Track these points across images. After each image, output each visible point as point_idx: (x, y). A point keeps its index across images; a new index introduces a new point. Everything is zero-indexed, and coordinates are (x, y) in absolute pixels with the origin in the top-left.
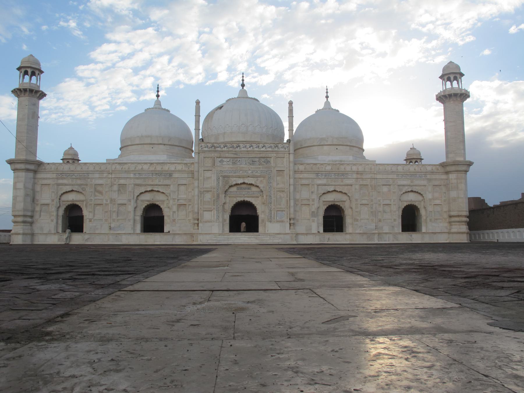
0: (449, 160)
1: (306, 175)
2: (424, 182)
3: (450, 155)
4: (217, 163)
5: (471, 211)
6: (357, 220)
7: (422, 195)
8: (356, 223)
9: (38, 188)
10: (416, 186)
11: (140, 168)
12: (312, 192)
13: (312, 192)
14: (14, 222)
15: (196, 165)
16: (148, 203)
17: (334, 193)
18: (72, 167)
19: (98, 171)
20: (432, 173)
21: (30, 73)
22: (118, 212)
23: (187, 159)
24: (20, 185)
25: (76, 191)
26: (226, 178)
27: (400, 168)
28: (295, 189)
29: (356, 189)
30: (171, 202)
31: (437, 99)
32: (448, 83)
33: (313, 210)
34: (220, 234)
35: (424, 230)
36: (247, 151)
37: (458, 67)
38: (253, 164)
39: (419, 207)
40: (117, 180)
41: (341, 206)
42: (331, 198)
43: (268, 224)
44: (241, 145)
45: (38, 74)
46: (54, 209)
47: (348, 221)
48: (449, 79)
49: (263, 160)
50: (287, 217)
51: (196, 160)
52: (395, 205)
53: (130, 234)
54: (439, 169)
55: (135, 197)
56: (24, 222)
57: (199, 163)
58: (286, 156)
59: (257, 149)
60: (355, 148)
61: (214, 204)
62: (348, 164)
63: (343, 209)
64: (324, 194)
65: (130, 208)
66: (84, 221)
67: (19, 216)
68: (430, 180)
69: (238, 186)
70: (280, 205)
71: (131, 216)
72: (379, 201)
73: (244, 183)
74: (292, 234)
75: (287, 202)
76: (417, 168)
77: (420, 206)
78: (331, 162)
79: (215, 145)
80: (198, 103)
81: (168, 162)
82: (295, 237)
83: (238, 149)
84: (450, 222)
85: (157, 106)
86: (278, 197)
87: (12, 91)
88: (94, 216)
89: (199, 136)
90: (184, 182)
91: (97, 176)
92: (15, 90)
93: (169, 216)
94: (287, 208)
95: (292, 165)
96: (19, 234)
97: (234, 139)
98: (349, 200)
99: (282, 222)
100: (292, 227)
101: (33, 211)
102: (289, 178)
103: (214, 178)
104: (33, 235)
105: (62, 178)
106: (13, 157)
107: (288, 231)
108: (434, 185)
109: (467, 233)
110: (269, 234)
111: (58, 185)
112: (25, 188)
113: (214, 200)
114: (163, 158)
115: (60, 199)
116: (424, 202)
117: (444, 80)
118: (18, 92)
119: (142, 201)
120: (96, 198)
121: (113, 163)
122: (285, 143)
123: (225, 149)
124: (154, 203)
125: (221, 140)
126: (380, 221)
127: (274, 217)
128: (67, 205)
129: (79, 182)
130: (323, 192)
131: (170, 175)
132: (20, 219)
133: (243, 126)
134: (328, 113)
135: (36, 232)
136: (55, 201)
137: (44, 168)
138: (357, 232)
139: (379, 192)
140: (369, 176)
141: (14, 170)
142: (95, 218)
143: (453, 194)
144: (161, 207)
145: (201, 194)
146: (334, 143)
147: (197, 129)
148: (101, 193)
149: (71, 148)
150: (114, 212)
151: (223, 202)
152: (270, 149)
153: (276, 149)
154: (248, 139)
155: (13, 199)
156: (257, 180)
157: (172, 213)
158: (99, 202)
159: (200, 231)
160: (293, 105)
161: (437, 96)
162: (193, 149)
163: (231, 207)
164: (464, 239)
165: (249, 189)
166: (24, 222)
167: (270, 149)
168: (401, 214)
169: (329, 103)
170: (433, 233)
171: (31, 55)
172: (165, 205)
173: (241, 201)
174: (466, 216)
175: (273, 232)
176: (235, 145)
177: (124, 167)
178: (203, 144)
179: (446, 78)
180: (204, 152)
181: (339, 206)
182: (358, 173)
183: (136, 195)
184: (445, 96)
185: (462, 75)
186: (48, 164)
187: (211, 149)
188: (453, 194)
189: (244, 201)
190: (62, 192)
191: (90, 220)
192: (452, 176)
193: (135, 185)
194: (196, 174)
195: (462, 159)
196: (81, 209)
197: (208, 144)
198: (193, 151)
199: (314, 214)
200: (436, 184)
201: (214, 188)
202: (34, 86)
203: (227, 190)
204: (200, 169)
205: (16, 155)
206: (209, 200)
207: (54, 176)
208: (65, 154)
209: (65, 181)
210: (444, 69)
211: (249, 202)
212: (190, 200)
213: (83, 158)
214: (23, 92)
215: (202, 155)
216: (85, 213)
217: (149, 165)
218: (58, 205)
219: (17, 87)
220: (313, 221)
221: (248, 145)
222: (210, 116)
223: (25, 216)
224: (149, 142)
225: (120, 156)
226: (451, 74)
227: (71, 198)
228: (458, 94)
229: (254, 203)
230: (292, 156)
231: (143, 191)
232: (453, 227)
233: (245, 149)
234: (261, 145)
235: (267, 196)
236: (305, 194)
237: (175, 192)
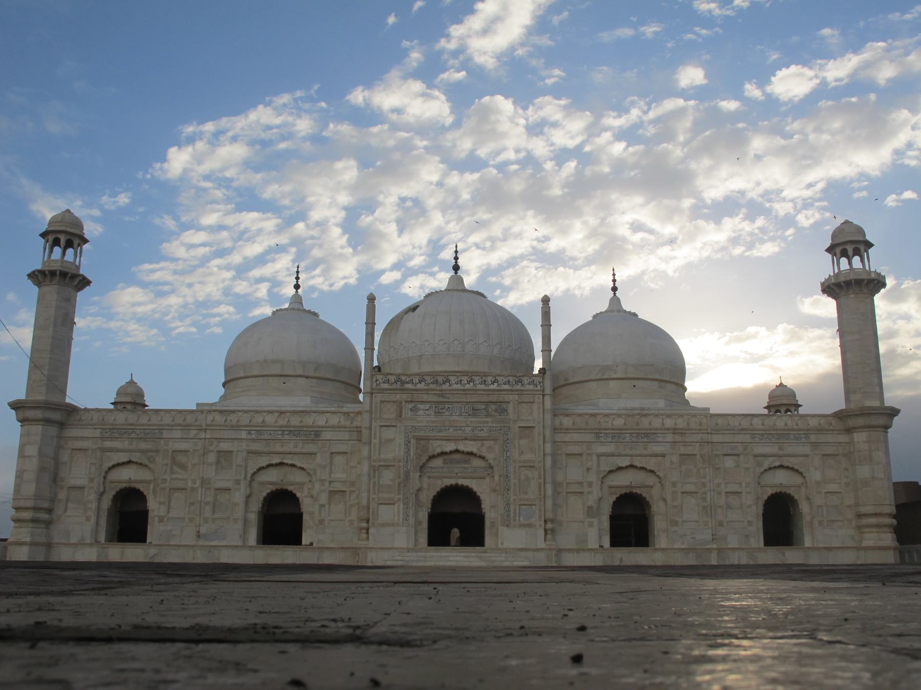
0: (852, 406)
1: (575, 437)
2: (806, 450)
3: (853, 397)
4: (407, 413)
5: (898, 507)
6: (675, 523)
7: (801, 473)
8: (675, 528)
9: (65, 457)
10: (789, 456)
11: (260, 420)
12: (588, 469)
13: (588, 469)
14: (16, 520)
15: (366, 416)
16: (274, 488)
17: (631, 471)
18: (132, 418)
19: (180, 425)
20: (819, 430)
21: (63, 242)
22: (214, 505)
23: (349, 405)
24: (32, 450)
25: (137, 463)
27: (757, 422)
28: (554, 463)
29: (672, 463)
30: (317, 486)
32: (844, 261)
33: (590, 503)
34: (409, 550)
35: (808, 542)
36: (464, 390)
37: (860, 231)
38: (474, 415)
39: (796, 497)
40: (215, 443)
41: (644, 495)
42: (624, 481)
43: (504, 532)
44: (452, 379)
45: (79, 245)
46: (93, 497)
47: (659, 524)
48: (844, 254)
49: (493, 407)
50: (540, 517)
51: (367, 407)
52: (749, 493)
53: (236, 547)
54: (833, 422)
55: (249, 476)
56: (34, 521)
57: (371, 412)
58: (538, 399)
59: (482, 387)
60: (668, 385)
61: (399, 490)
62: (657, 416)
63: (648, 502)
64: (611, 472)
65: (239, 497)
66: (150, 521)
67: (26, 509)
68: (815, 445)
69: (446, 457)
70: (526, 493)
71: (240, 512)
72: (719, 485)
73: (457, 451)
74: (550, 549)
76: (789, 423)
77: (799, 496)
78: (623, 412)
79: (403, 378)
80: (371, 299)
81: (314, 409)
82: (556, 555)
83: (446, 387)
84: (859, 528)
85: (296, 306)
87: (29, 276)
88: (168, 512)
89: (372, 360)
90: (344, 448)
91: (178, 434)
92: (33, 272)
93: (311, 514)
94: (540, 500)
95: (548, 416)
96: (22, 544)
97: (438, 368)
98: (658, 485)
99: (530, 526)
100: (549, 536)
101: (53, 500)
102: (544, 442)
104: (49, 546)
105: (112, 439)
106: (22, 397)
107: (542, 545)
108: (824, 455)
109: (895, 549)
110: (506, 551)
111: (104, 450)
112: (41, 454)
114: (303, 402)
115: (105, 478)
116: (807, 487)
117: (835, 254)
118: (39, 277)
119: (262, 484)
120: (175, 476)
121: (209, 411)
122: (535, 375)
123: (422, 386)
124: (285, 487)
125: (414, 369)
126: (721, 524)
127: (514, 517)
128: (118, 489)
129: (143, 445)
130: (608, 469)
131: (315, 434)
132: (27, 515)
133: (456, 342)
134: (616, 317)
135: (56, 540)
136: (96, 481)
137: (78, 417)
138: (676, 546)
139: (718, 469)
140: (698, 438)
141: (23, 421)
142: (170, 515)
143: (864, 472)
144: (298, 495)
145: (374, 472)
146: (629, 375)
147: (369, 348)
148: (183, 467)
149: (132, 383)
150: (207, 503)
151: (417, 488)
152: (507, 387)
153: (519, 387)
154: (465, 368)
155: (17, 477)
156: (482, 445)
157: (317, 507)
158: (179, 484)
159: (371, 543)
161: (822, 284)
162: (362, 386)
163: (431, 497)
164: (890, 558)
165: (466, 462)
166: (34, 521)
167: (507, 387)
168: (761, 512)
169: (618, 300)
170: (826, 548)
171: (68, 211)
172: (306, 492)
173: (451, 485)
174: (890, 515)
175: (512, 546)
176: (440, 379)
177: (229, 418)
178: (379, 377)
179: (838, 250)
181: (641, 495)
182: (675, 431)
183: (251, 472)
184: (838, 285)
185: (869, 245)
186: (86, 410)
187: (394, 386)
188: (864, 472)
189: (457, 485)
190: (110, 464)
191: (161, 520)
192: (860, 437)
193: (249, 452)
194: (365, 433)
195: (876, 404)
196: (145, 497)
197: (389, 377)
198: (360, 391)
199: (591, 512)
200: (828, 452)
201: (400, 461)
203: (424, 464)
204: (374, 424)
205: (27, 394)
206: (390, 483)
207: (97, 433)
208: (119, 393)
209: (116, 444)
210: (834, 237)
211: (467, 487)
212: (353, 484)
213: (152, 402)
214: (49, 277)
215: (378, 398)
216: (153, 506)
217: (277, 415)
218: (102, 489)
219: (39, 267)
220: (591, 525)
221: (465, 379)
222: (394, 325)
223: (36, 509)
224: (278, 371)
225: (223, 398)
226: (849, 243)
227: (127, 476)
228: (863, 280)
229: (475, 489)
230: (548, 401)
231: (264, 465)
232: (866, 535)
233: (459, 387)
234: (489, 379)
235: (500, 476)
236: (573, 472)
237: (324, 467)
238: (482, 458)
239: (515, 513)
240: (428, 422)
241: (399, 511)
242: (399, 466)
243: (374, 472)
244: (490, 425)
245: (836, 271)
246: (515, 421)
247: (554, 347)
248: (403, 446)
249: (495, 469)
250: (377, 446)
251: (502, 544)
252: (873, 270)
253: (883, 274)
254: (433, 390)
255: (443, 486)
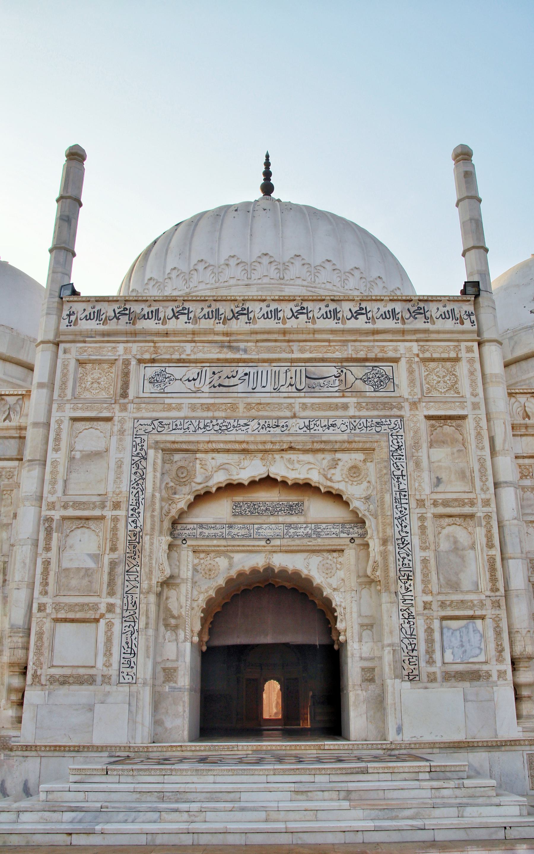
26: (177, 457)
36: (284, 332)
44: (255, 308)
49: (359, 371)
50: (500, 651)
58: (467, 352)
61: (111, 583)
73: (268, 482)
75: (492, 569)
79: (136, 308)
86: (444, 546)
94: (496, 605)
103: (122, 452)
107: (509, 728)
113: (113, 565)
127: (430, 652)
145: (49, 532)
151: (157, 577)
152: (390, 324)
163: (201, 602)
165: (292, 509)
173: (254, 571)
175: (428, 738)
178: (78, 307)
180: (83, 337)
187: (112, 326)
189: (269, 569)
201: (117, 506)
203: (182, 513)
204: (55, 415)
206: (91, 564)
211: (297, 574)
235: (385, 542)
238: (336, 497)
239: (430, 641)
240: (193, 408)
241: (109, 640)
242: (115, 519)
243: (49, 532)
244: (352, 412)
246: (414, 405)
248: (126, 467)
249: (370, 523)
250: (61, 469)
251: (399, 730)
254: (206, 332)
255: (233, 573)
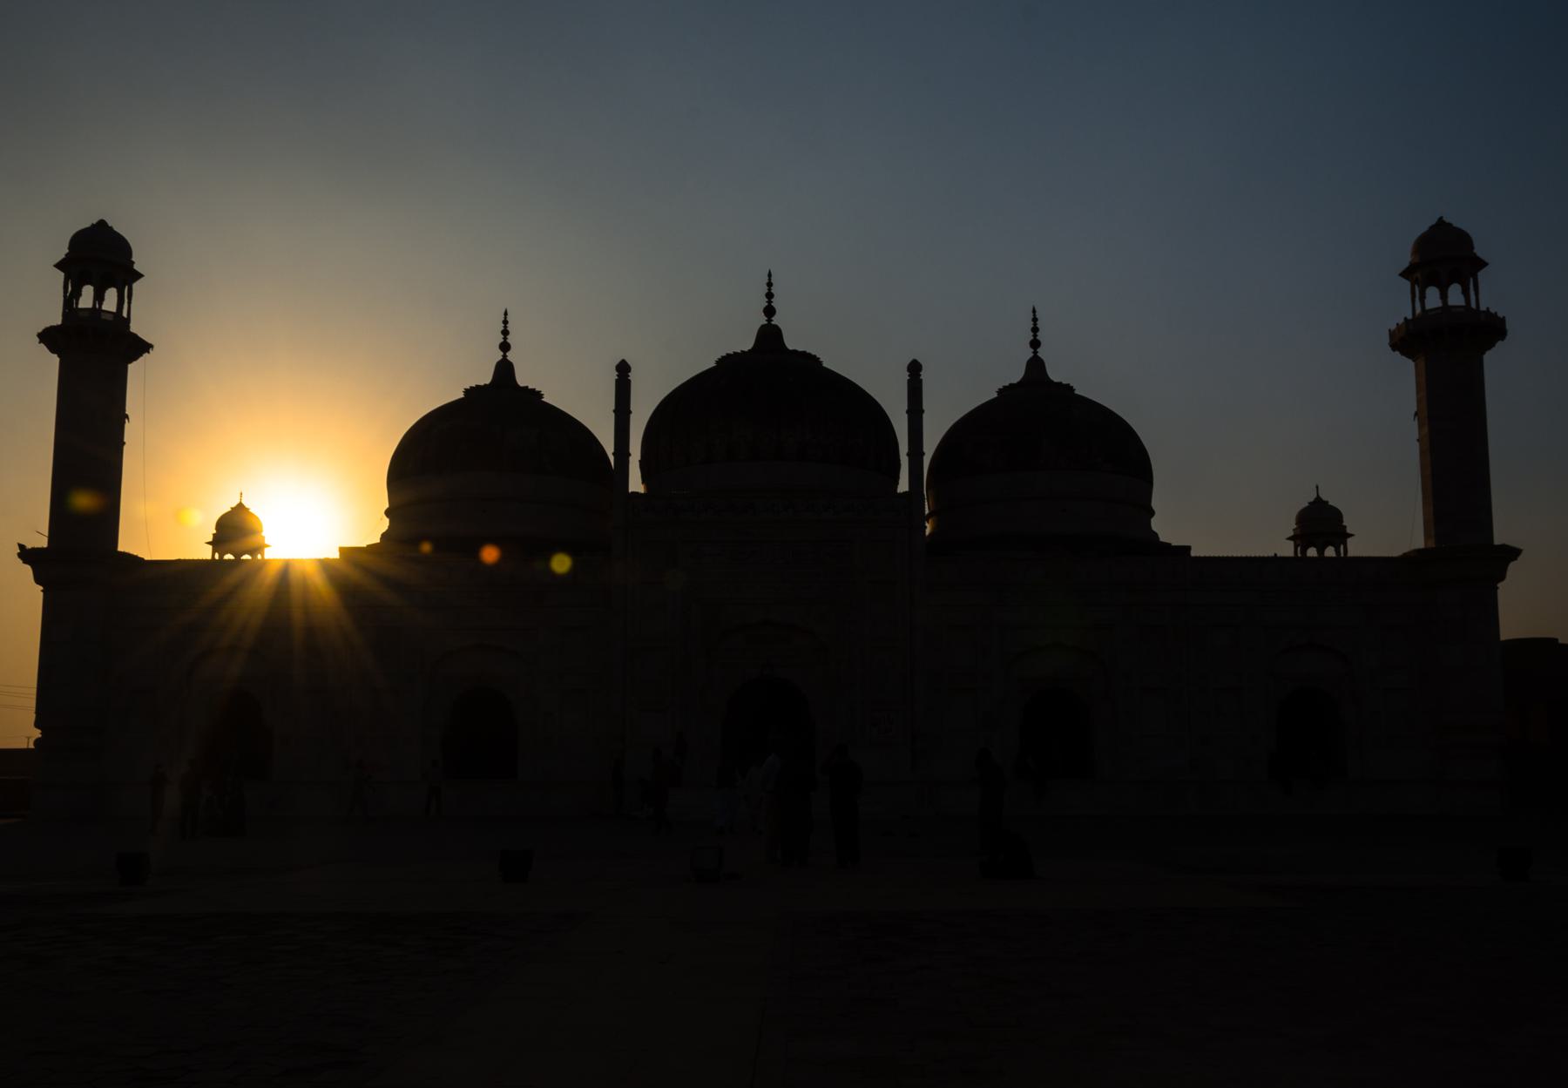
31: (1394, 347)
80: (623, 369)
160: (924, 375)
161: (1392, 334)
171: (102, 223)
202: (110, 318)
245: (1418, 310)
247: (930, 447)
252: (1483, 308)
253: (1500, 315)
